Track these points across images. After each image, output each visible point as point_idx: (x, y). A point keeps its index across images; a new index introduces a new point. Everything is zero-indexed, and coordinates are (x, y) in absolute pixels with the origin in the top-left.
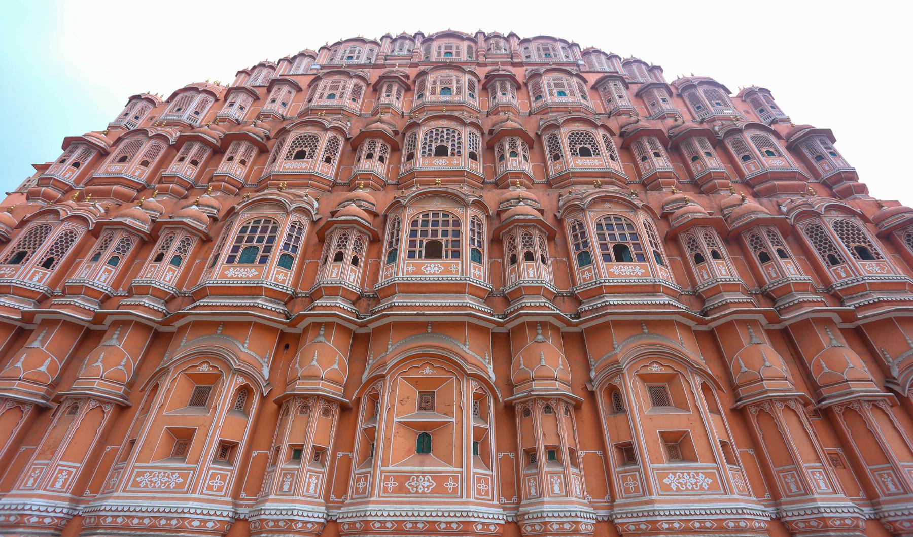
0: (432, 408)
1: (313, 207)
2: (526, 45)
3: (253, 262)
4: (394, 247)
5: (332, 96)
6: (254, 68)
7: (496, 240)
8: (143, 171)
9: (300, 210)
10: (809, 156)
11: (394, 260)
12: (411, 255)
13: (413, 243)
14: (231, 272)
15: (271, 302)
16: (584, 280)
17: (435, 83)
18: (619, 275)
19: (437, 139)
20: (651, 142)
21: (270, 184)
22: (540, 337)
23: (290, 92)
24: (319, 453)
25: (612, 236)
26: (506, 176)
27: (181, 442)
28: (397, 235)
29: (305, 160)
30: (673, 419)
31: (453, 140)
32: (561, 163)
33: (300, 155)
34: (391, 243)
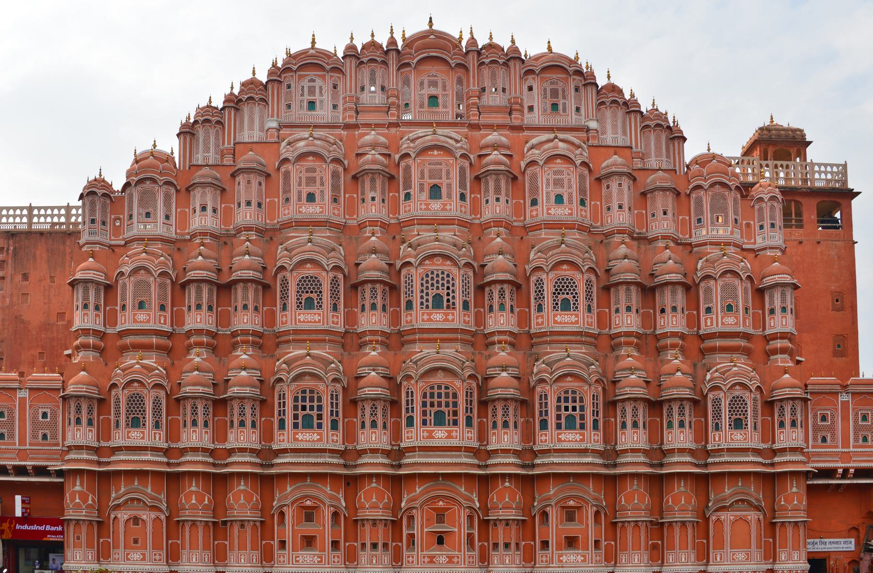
0: (444, 522)
1: (340, 372)
2: (531, 80)
3: (312, 427)
4: (410, 414)
5: (311, 198)
6: (196, 122)
7: (484, 404)
8: (165, 317)
9: (335, 380)
10: (767, 306)
11: (412, 425)
12: (424, 423)
13: (424, 413)
14: (300, 436)
15: (332, 457)
16: (542, 441)
17: (422, 177)
18: (565, 441)
19: (432, 285)
20: (628, 289)
21: (293, 340)
22: (507, 484)
23: (260, 184)
24: (385, 545)
25: (566, 409)
26: (493, 334)
27: (309, 542)
28: (412, 404)
29: (315, 311)
30: (573, 528)
31: (448, 288)
32: (542, 317)
33: (309, 304)
34: (407, 409)
